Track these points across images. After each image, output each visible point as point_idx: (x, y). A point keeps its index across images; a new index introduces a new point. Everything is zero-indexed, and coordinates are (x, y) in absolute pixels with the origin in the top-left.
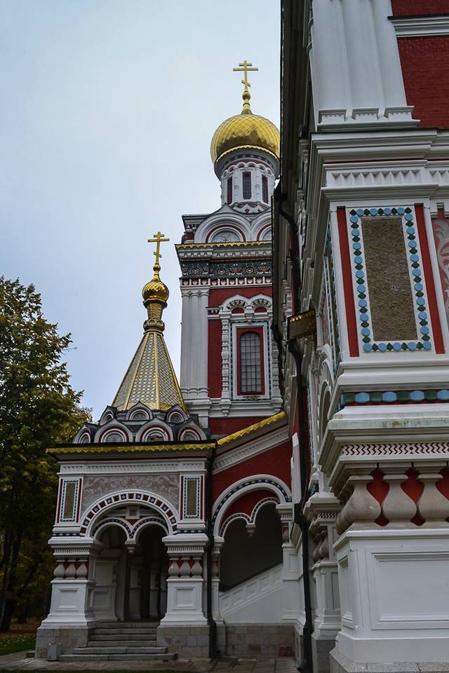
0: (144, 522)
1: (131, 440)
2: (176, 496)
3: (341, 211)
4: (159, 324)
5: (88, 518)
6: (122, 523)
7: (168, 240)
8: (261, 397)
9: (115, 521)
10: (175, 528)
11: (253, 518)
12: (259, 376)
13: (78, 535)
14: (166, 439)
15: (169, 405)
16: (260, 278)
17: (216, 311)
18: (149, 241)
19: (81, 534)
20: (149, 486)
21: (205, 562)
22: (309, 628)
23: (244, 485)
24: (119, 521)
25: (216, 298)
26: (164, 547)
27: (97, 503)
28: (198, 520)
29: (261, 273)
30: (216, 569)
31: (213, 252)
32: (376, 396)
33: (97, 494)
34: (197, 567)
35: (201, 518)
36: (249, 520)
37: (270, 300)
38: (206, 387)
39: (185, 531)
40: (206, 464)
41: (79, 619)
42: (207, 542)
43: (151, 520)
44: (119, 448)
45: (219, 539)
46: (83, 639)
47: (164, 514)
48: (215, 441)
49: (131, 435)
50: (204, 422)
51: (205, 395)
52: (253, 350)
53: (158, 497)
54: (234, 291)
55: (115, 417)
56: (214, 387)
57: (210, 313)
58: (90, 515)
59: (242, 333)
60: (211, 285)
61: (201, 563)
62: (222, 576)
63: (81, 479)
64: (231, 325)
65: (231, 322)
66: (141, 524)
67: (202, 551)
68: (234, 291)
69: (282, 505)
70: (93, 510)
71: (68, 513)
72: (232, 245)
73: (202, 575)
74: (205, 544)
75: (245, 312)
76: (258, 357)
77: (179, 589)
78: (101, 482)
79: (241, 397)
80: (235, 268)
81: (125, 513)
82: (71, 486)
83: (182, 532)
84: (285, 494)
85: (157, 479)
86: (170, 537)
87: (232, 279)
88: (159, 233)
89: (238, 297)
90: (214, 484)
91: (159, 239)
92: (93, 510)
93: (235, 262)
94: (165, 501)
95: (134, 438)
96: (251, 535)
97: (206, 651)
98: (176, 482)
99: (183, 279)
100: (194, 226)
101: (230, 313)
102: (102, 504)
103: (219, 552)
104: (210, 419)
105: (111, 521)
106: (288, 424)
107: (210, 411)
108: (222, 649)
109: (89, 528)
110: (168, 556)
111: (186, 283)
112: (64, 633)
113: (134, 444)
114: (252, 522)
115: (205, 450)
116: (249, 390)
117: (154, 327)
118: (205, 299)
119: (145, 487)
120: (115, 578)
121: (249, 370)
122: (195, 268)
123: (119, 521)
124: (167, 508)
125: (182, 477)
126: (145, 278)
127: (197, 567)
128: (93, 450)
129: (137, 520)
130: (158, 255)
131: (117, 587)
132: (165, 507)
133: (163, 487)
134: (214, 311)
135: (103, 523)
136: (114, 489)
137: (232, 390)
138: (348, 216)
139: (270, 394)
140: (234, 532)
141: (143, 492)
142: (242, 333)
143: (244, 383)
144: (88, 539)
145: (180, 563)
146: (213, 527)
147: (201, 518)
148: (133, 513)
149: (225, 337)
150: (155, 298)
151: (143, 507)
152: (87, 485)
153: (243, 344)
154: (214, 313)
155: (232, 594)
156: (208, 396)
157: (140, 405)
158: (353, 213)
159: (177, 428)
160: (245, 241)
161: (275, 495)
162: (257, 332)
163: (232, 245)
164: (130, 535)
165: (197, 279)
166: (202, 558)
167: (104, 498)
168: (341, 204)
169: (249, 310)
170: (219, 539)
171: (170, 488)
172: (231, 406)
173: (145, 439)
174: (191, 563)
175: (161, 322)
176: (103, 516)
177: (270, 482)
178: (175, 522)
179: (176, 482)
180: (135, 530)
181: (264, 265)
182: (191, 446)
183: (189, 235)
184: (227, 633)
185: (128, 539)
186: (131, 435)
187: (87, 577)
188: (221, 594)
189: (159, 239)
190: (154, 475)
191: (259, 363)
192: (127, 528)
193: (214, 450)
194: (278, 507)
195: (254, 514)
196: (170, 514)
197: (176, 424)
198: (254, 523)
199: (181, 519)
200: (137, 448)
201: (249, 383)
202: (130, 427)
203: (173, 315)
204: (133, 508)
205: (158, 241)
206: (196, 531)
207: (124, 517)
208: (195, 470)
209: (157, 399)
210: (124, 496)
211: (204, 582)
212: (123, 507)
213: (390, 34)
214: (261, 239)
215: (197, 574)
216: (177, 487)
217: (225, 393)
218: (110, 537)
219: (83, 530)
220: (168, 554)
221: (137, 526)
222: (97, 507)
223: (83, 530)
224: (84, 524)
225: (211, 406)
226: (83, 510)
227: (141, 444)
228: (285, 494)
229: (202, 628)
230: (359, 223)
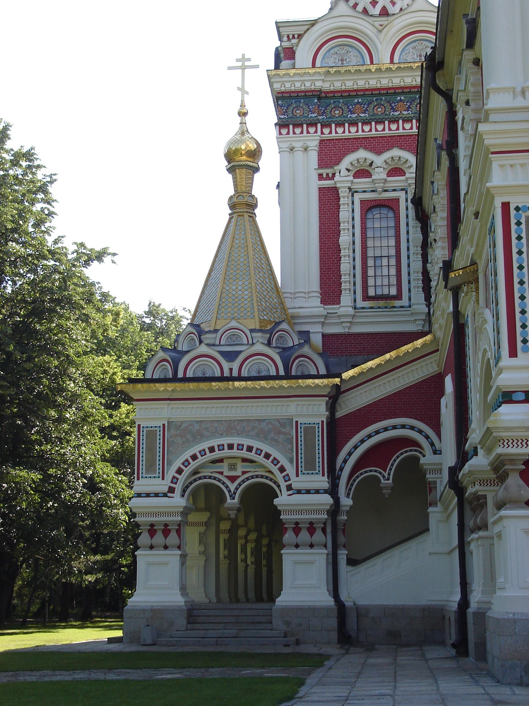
0: (248, 479)
1: (227, 374)
2: (290, 446)
3: (506, 206)
4: (250, 200)
5: (177, 476)
6: (219, 480)
7: (257, 67)
8: (397, 303)
9: (210, 477)
10: (289, 488)
11: (389, 474)
12: (393, 271)
13: (165, 495)
14: (273, 372)
15: (271, 322)
16: (395, 120)
17: (330, 175)
18: (230, 68)
19: (169, 495)
20: (253, 433)
21: (329, 529)
22: (464, 603)
23: (377, 432)
24: (215, 478)
25: (330, 154)
27: (187, 455)
28: (319, 477)
29: (396, 113)
30: (342, 539)
31: (323, 81)
33: (187, 444)
34: (319, 536)
35: (323, 475)
36: (384, 477)
37: (412, 159)
38: (319, 290)
40: (327, 403)
41: (174, 598)
42: (331, 506)
43: (257, 476)
44: (214, 384)
45: (346, 502)
46: (182, 622)
48: (339, 375)
49: (226, 366)
50: (317, 340)
51: (317, 302)
52: (384, 233)
53: (266, 448)
54: (353, 144)
55: (201, 342)
56: (330, 291)
57: (321, 177)
58: (180, 471)
59: (369, 207)
60: (322, 133)
61: (324, 530)
63: (164, 425)
64: (353, 196)
65: (352, 192)
66: (243, 481)
67: (326, 516)
68: (353, 144)
69: (428, 459)
70: (183, 464)
71: (151, 468)
72: (353, 69)
73: (325, 546)
74: (329, 507)
75: (373, 177)
76: (392, 242)
77: (296, 563)
78: (190, 428)
79: (367, 304)
80: (358, 106)
81: (222, 467)
82: (151, 434)
83: (299, 492)
84: (432, 444)
85: (263, 425)
86: (283, 500)
87: (354, 123)
88: (243, 55)
89: (362, 154)
90: (338, 430)
91: (244, 64)
92: (183, 464)
93: (357, 96)
94: (275, 453)
95: (231, 370)
96: (387, 496)
97: (334, 635)
98: (288, 428)
99: (281, 125)
100: (294, 37)
101: (351, 178)
102: (194, 457)
103: (345, 518)
104: (325, 336)
105: (205, 477)
106: (438, 350)
107: (323, 324)
108: (353, 634)
109: (178, 488)
110: (281, 523)
111: (284, 131)
112: (156, 614)
113: (231, 379)
114: (388, 479)
115: (326, 386)
116: (379, 292)
117: (243, 206)
118: (314, 156)
119: (248, 436)
120: (202, 549)
121: (378, 263)
122: (297, 107)
123: (215, 478)
124: (278, 462)
125: (297, 422)
126: (227, 131)
127: (319, 536)
128: (178, 386)
129: (238, 477)
130: (243, 90)
131: (206, 560)
132: (275, 461)
133: (272, 435)
134: (327, 174)
135: (195, 480)
136: (208, 438)
137: (355, 293)
138: (513, 212)
139: (410, 299)
140: (366, 491)
141: (247, 442)
142: (369, 207)
143: (371, 282)
144: (178, 501)
145: (297, 530)
146: (338, 486)
147: (323, 475)
149: (344, 214)
150: (242, 162)
151: (244, 460)
152: (173, 432)
153: (369, 224)
154: (328, 178)
155: (362, 568)
156: (322, 302)
157: (234, 324)
158: (517, 209)
159: (287, 355)
160: (372, 63)
161: (416, 444)
162: (391, 205)
163: (353, 69)
164: (231, 496)
165: (301, 125)
166: (325, 524)
167: (195, 450)
168: (506, 200)
169: (379, 174)
171: (281, 437)
172: (354, 316)
173: (244, 373)
174: (311, 529)
175: (253, 197)
176: (195, 472)
177: (412, 428)
178: (289, 480)
179: (288, 428)
180: (237, 489)
181: (401, 100)
182: (310, 381)
183: (284, 55)
184: (358, 616)
185: (229, 500)
186: (226, 366)
187: (179, 548)
188: (350, 568)
189: (244, 64)
191: (393, 252)
192: (227, 487)
193: (337, 386)
194: (422, 460)
195: (390, 469)
196: (282, 469)
197: (284, 349)
198: (391, 481)
199: (297, 475)
200: (237, 384)
201: (379, 283)
202: (224, 354)
203: (265, 186)
205: (243, 68)
206: (317, 492)
207: (222, 473)
208: (315, 413)
209: (256, 314)
210: (221, 447)
211: (328, 554)
212: (221, 460)
214: (396, 60)
215: (319, 545)
216: (290, 434)
217: (346, 299)
218: (206, 496)
219: (172, 490)
220: (282, 520)
221: (240, 485)
222: (187, 460)
223: (172, 490)
224: (172, 482)
225: (326, 317)
226: (170, 464)
227: (240, 378)
228: (432, 444)
229: (328, 609)
230: (523, 220)
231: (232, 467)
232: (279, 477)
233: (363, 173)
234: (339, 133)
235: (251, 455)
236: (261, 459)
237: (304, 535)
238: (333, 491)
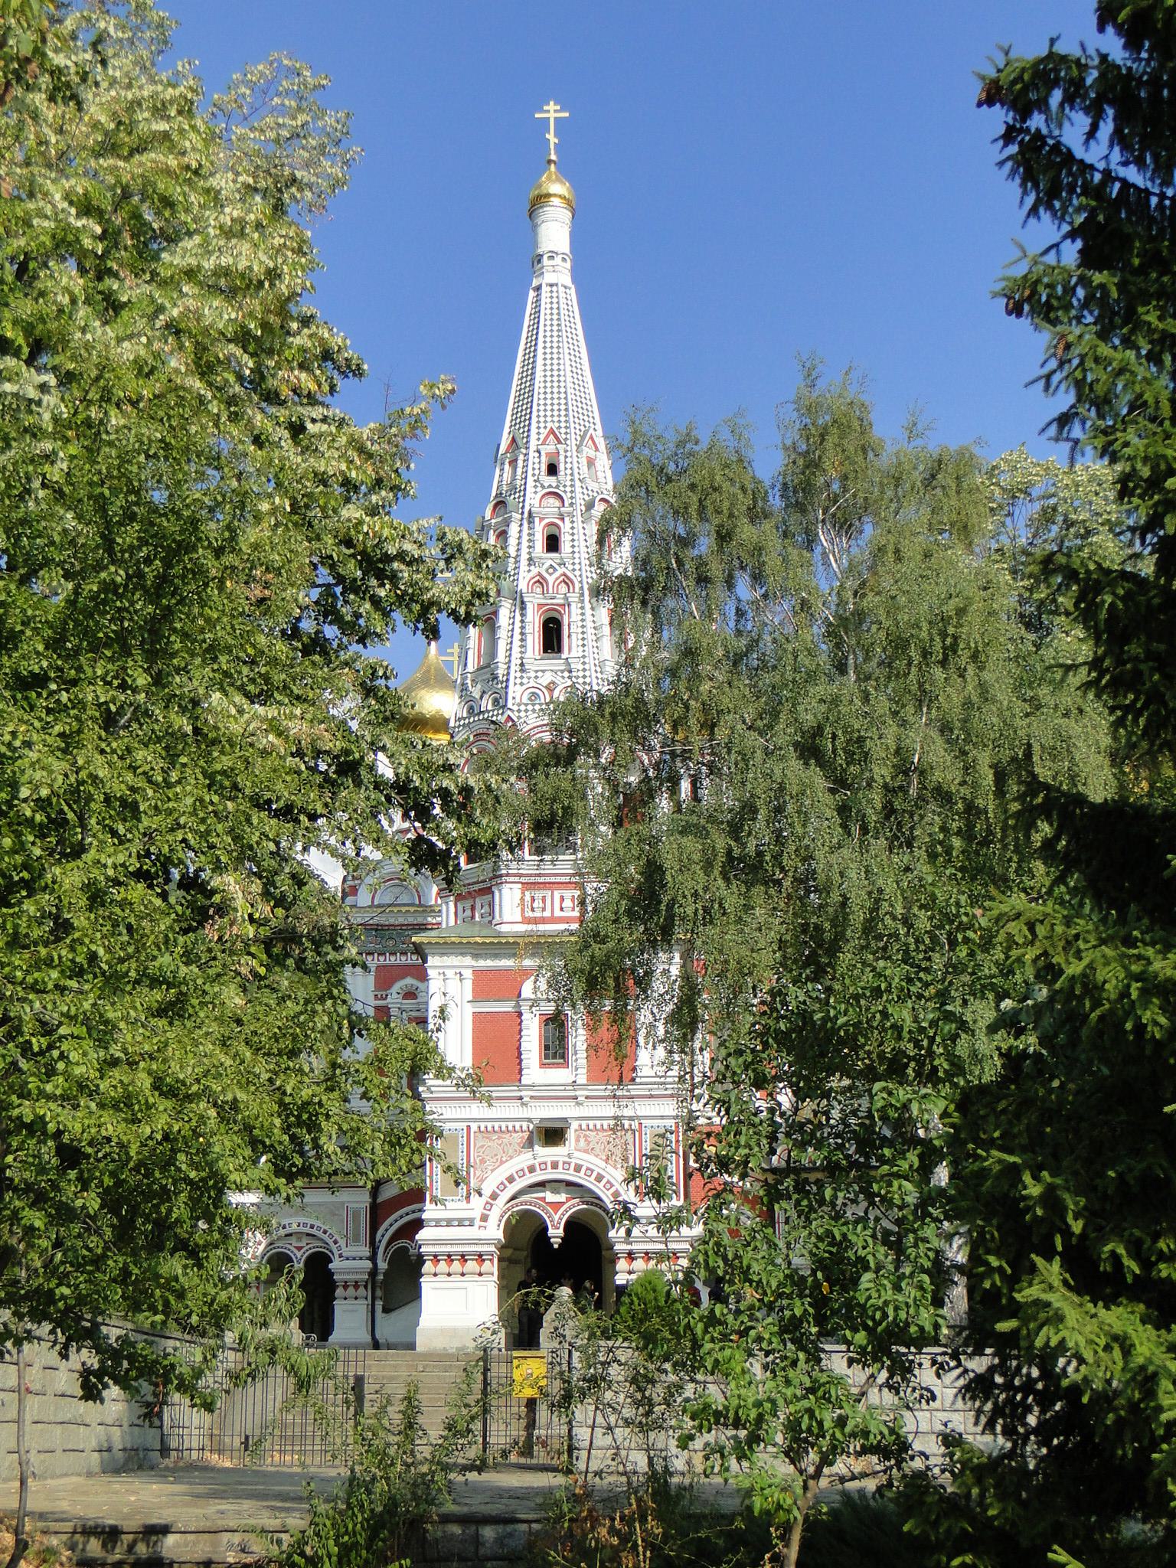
26: (331, 1274)
30: (379, 1293)
32: (438, 1223)
34: (362, 1290)
39: (350, 1261)
45: (383, 1265)
47: (330, 1242)
62: (385, 1299)
89: (409, 981)
90: (377, 1213)
127: (362, 1290)
145: (346, 1287)
148: (299, 1239)
155: (393, 1315)
170: (383, 1265)
174: (356, 1286)
190: (320, 1205)
204: (299, 1235)
213: (469, 1010)
231: (299, 1239)
232: (334, 1247)
233: (410, 995)
234: (392, 960)
235: (313, 1231)
236: (320, 1234)
237: (351, 1291)
238: (373, 1258)
